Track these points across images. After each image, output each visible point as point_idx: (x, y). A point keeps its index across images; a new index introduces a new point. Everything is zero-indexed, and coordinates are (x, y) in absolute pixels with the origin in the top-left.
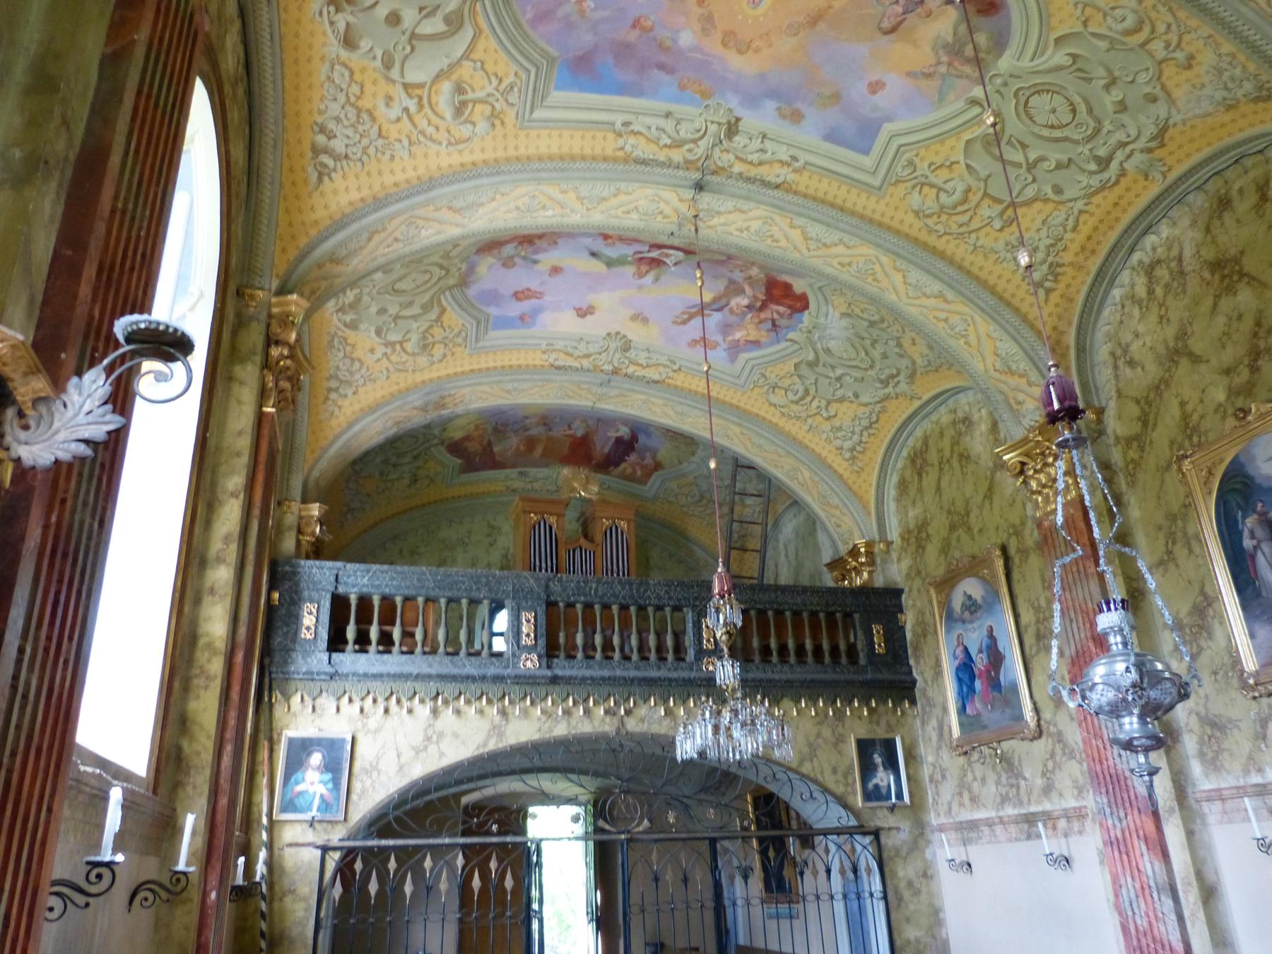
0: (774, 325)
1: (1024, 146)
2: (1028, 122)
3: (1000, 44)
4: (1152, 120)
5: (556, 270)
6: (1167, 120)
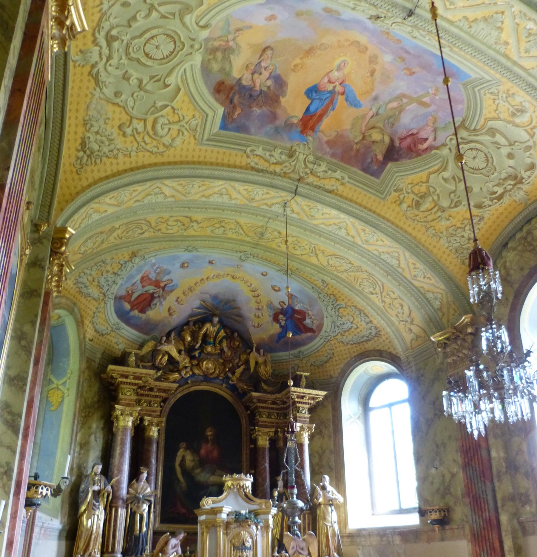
1: (163, 17)
2: (168, 32)
3: (206, 70)
4: (107, 83)
6: (101, 89)
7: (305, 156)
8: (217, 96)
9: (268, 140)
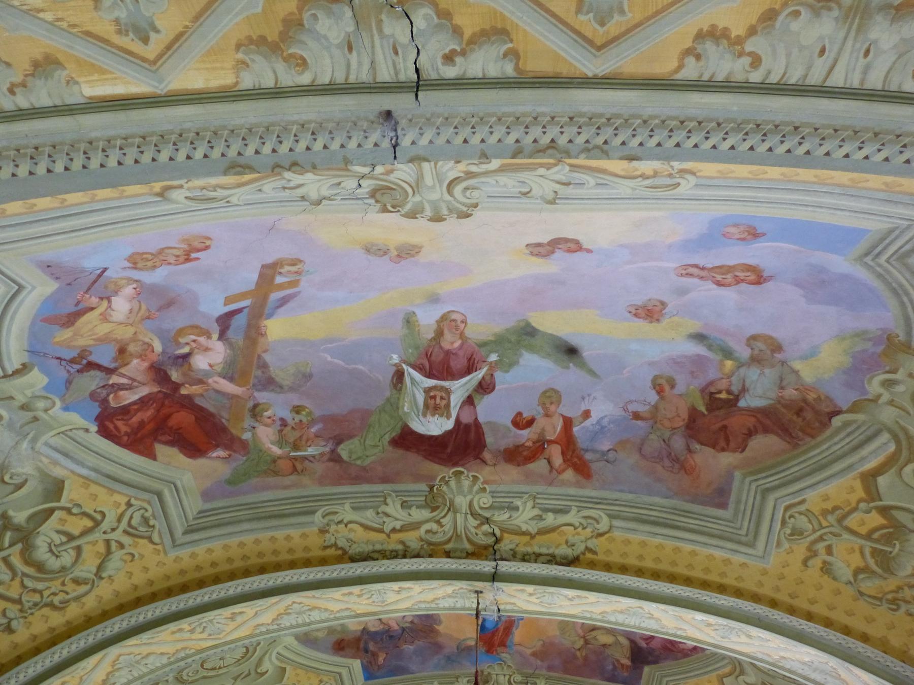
0: (92, 366)
5: (650, 312)
7: (507, 677)
8: (342, 653)
9: (443, 672)
